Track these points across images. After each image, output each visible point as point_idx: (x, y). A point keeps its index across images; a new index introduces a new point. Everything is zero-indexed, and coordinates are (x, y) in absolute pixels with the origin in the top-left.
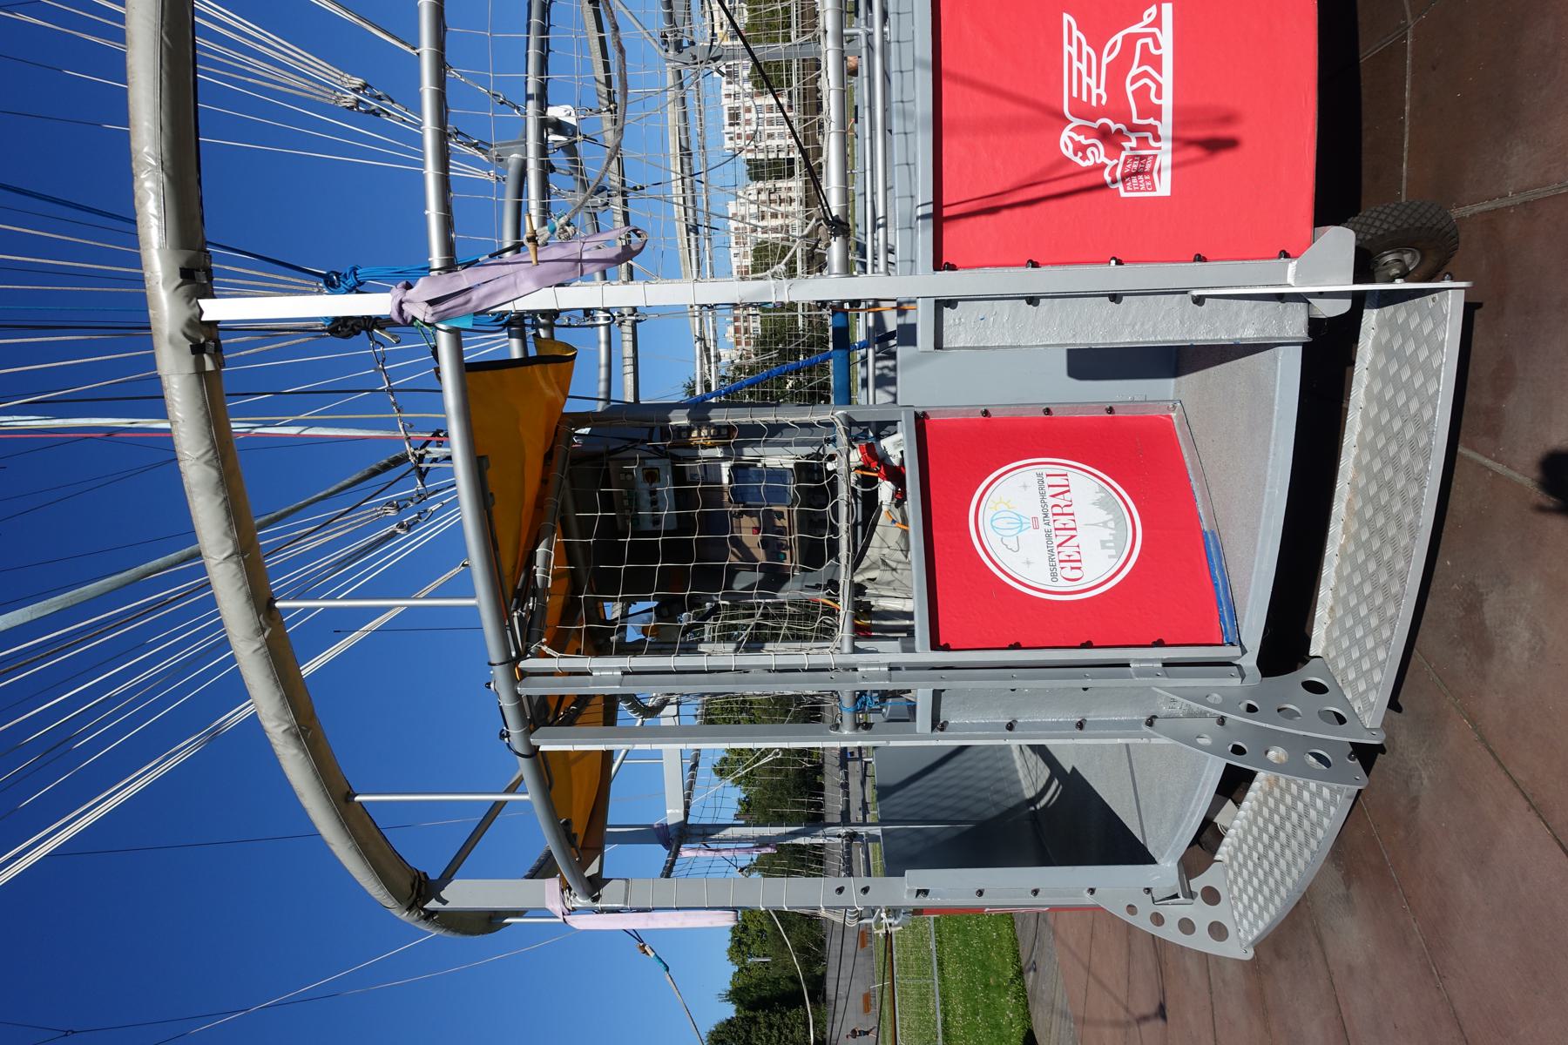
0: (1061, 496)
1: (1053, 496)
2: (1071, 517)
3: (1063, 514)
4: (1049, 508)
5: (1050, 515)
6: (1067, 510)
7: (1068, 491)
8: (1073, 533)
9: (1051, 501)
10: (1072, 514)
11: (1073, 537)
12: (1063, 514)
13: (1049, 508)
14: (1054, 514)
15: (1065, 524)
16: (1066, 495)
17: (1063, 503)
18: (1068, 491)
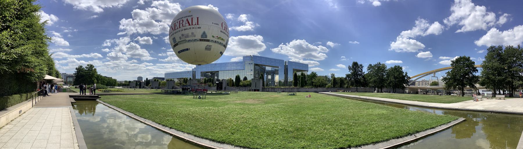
0: (187, 22)
1: (187, 20)
2: (179, 27)
3: (180, 24)
4: (181, 19)
5: (180, 20)
6: (181, 25)
7: (189, 25)
8: (174, 29)
9: (185, 19)
10: (180, 27)
11: (173, 29)
12: (180, 24)
13: (181, 19)
14: (180, 21)
15: (176, 26)
16: (188, 24)
17: (184, 24)
18: (189, 25)
